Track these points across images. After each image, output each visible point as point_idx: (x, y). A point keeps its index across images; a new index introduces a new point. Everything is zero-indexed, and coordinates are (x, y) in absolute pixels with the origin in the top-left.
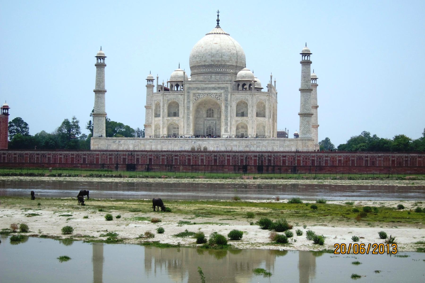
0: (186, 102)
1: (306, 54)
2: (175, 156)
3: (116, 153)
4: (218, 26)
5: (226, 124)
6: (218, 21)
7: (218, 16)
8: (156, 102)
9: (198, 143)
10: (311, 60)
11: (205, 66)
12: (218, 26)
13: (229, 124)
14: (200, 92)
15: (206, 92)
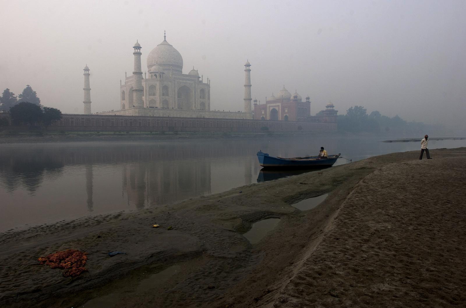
0: (173, 87)
1: (248, 65)
2: (197, 121)
3: (162, 119)
4: (165, 40)
5: (195, 103)
6: (165, 37)
7: (165, 34)
8: (150, 85)
9: (200, 113)
10: (250, 69)
11: (169, 65)
12: (165, 40)
13: (197, 103)
14: (181, 81)
15: (184, 81)
